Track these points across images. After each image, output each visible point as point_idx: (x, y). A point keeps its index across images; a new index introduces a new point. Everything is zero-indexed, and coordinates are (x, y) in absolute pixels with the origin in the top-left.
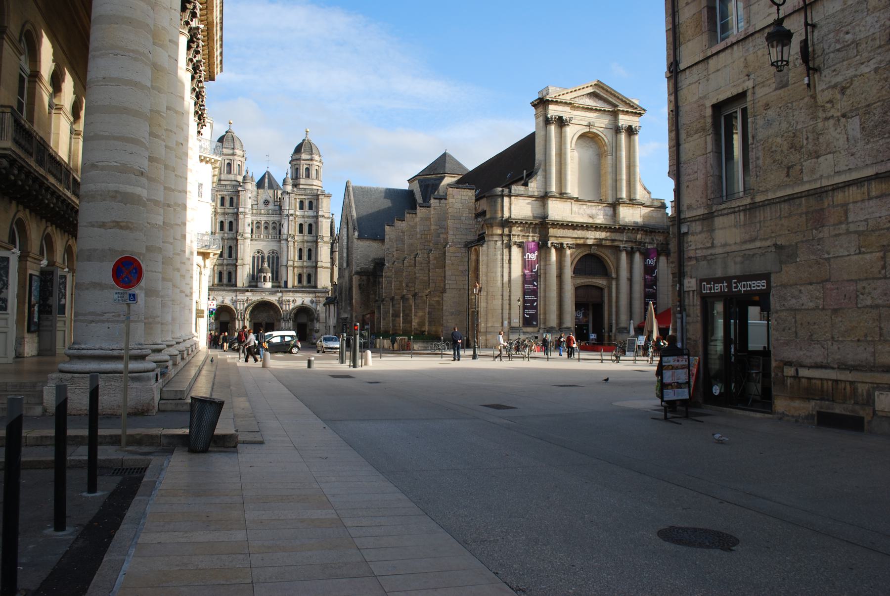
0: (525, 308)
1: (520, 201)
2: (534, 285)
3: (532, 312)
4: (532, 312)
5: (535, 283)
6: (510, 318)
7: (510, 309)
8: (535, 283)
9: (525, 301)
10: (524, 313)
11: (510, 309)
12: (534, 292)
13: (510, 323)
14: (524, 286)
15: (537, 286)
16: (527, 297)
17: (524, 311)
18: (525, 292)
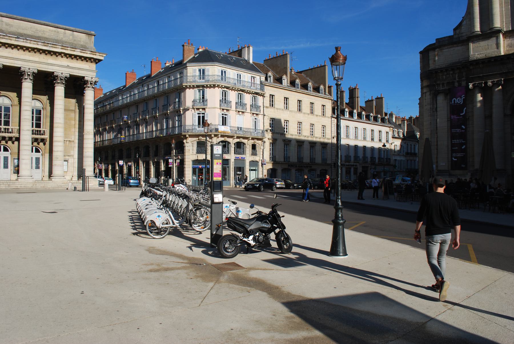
0: (453, 151)
1: (444, 50)
2: (462, 129)
3: (459, 155)
4: (459, 155)
5: (463, 127)
6: (437, 162)
7: (437, 154)
8: (463, 127)
9: (453, 145)
10: (452, 157)
11: (437, 154)
12: (463, 136)
13: (437, 166)
14: (451, 131)
15: (466, 129)
16: (456, 141)
17: (452, 155)
18: (453, 137)
